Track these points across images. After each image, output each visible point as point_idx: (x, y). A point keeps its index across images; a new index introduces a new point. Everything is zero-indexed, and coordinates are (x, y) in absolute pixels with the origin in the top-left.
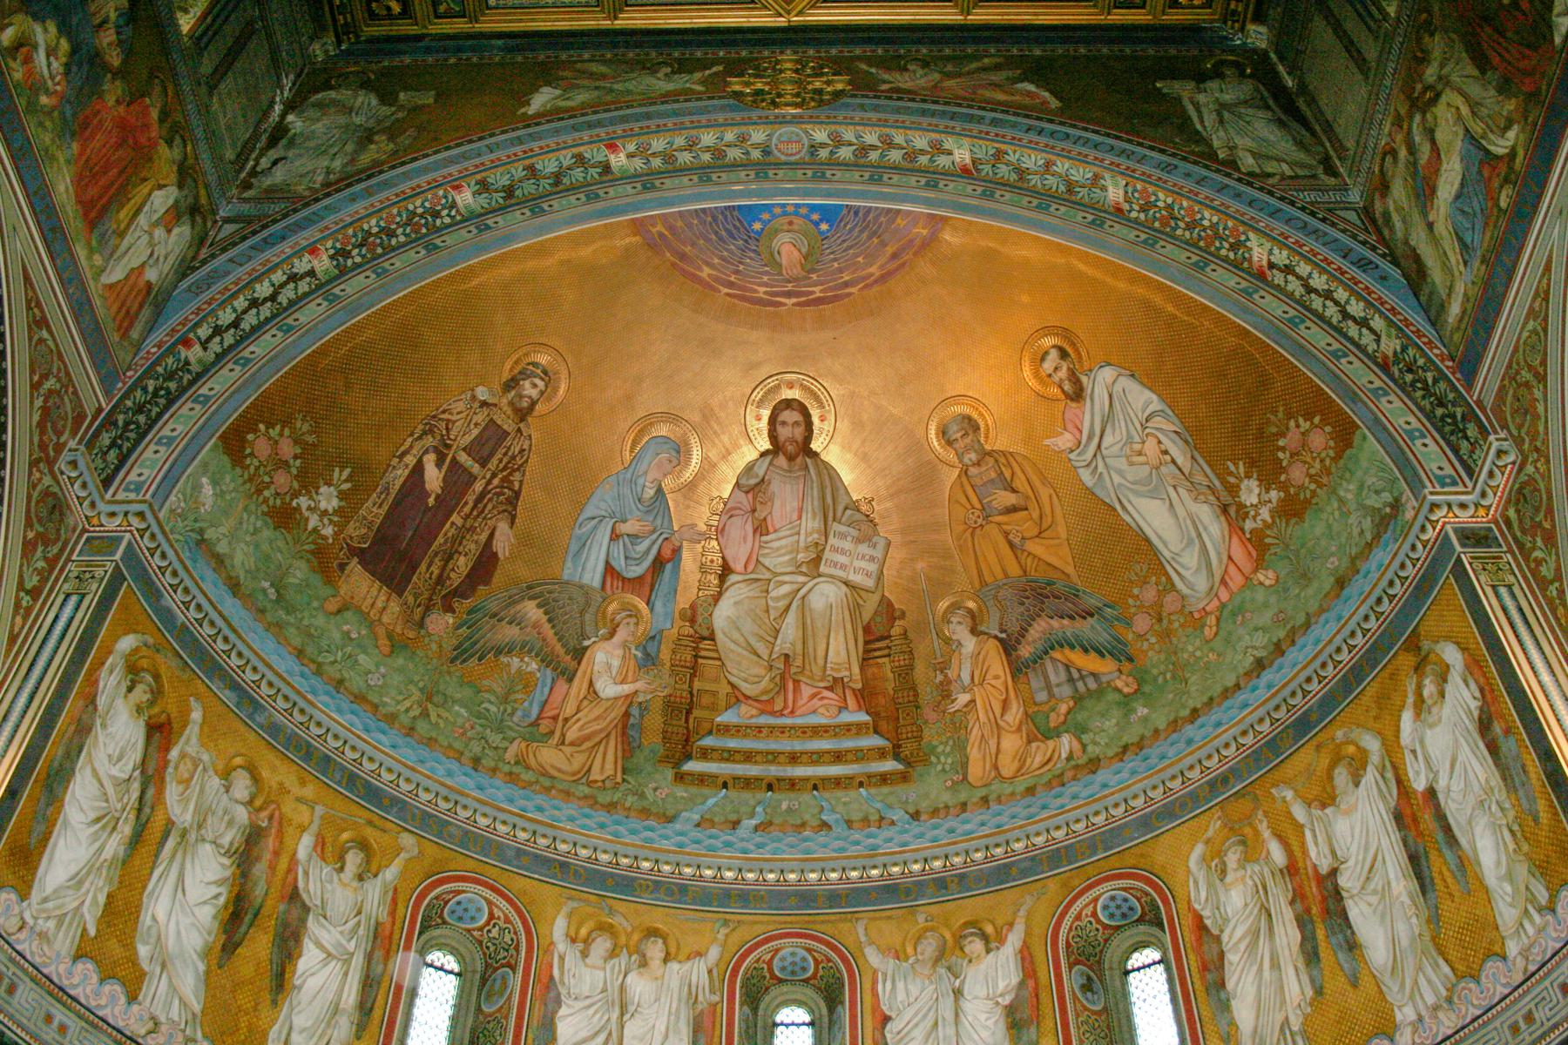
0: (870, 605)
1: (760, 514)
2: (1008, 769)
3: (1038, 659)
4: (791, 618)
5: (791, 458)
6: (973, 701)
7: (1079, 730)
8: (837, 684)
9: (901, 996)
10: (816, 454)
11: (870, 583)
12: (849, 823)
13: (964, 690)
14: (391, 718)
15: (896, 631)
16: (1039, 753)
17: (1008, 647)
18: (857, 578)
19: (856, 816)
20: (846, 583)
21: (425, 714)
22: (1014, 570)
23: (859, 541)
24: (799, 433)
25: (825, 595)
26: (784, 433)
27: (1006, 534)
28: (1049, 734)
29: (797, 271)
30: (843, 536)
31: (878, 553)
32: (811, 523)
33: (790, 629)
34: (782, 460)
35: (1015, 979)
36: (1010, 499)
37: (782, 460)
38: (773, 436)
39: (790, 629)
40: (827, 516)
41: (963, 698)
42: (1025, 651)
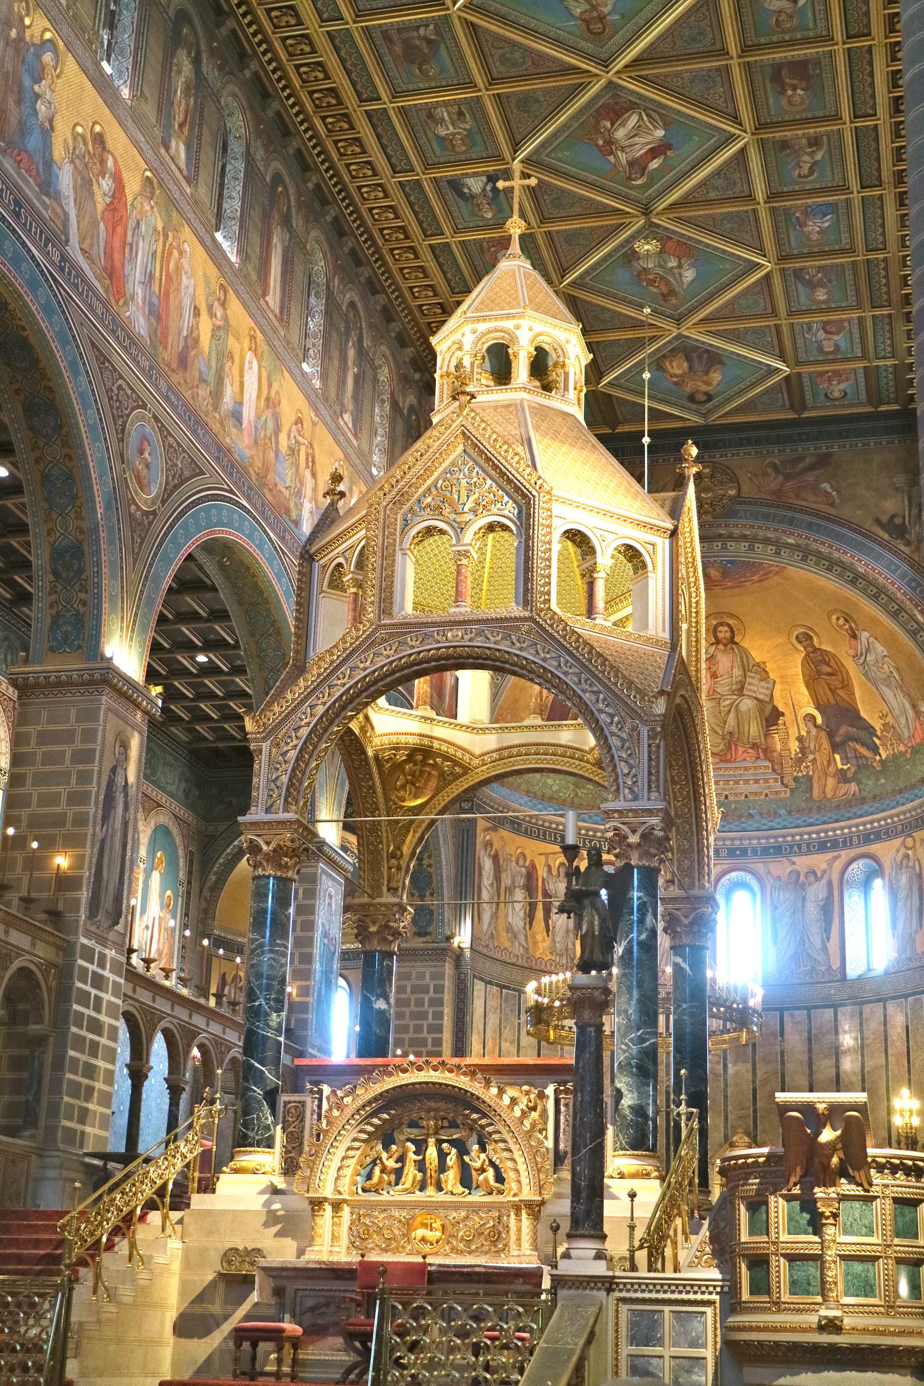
0: (768, 709)
1: (714, 669)
2: (829, 795)
3: (844, 742)
4: (732, 715)
5: (725, 645)
6: (815, 759)
7: (859, 783)
8: (754, 746)
9: (782, 897)
10: (736, 644)
11: (768, 699)
12: (761, 814)
13: (811, 753)
14: (564, 801)
15: (780, 722)
16: (843, 788)
17: (831, 735)
18: (761, 697)
19: (764, 811)
20: (756, 699)
21: (576, 794)
22: (832, 701)
23: (761, 680)
24: (728, 635)
25: (747, 704)
26: (720, 635)
27: (828, 684)
28: (847, 781)
29: (719, 578)
30: (753, 678)
31: (770, 686)
32: (737, 672)
33: (731, 720)
34: (721, 647)
35: (825, 895)
36: (829, 670)
37: (721, 647)
38: (716, 637)
39: (731, 720)
40: (745, 669)
41: (811, 757)
42: (838, 739)
